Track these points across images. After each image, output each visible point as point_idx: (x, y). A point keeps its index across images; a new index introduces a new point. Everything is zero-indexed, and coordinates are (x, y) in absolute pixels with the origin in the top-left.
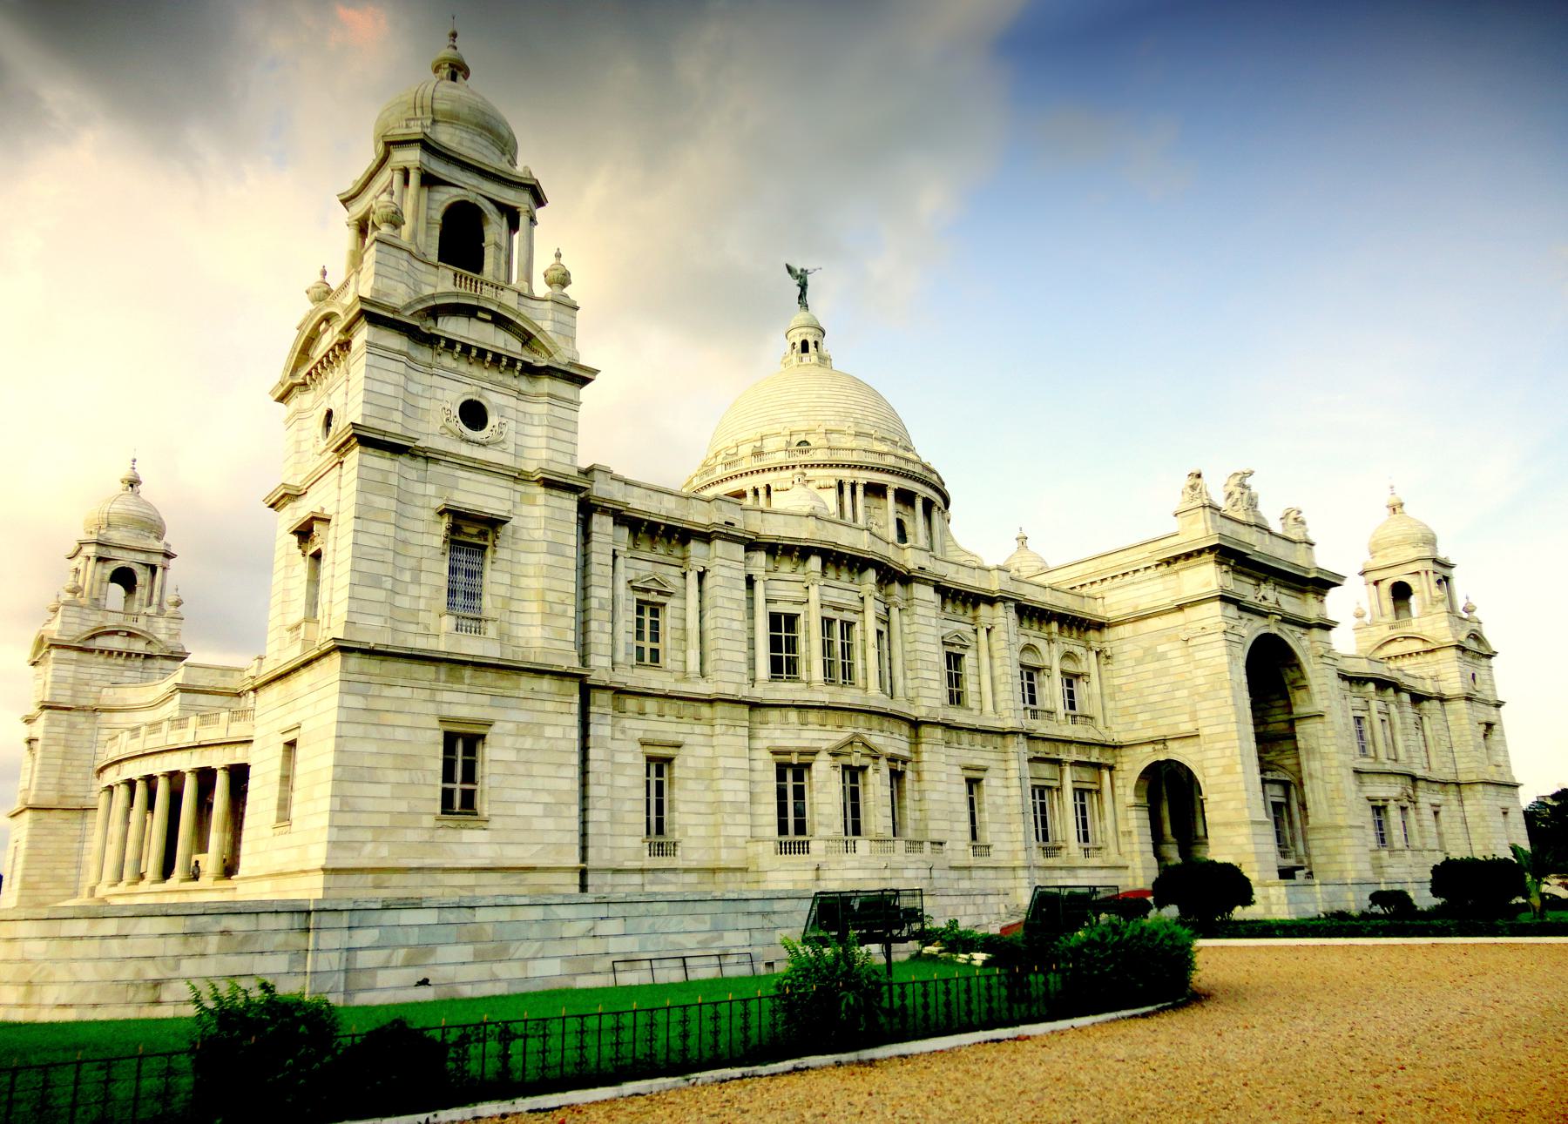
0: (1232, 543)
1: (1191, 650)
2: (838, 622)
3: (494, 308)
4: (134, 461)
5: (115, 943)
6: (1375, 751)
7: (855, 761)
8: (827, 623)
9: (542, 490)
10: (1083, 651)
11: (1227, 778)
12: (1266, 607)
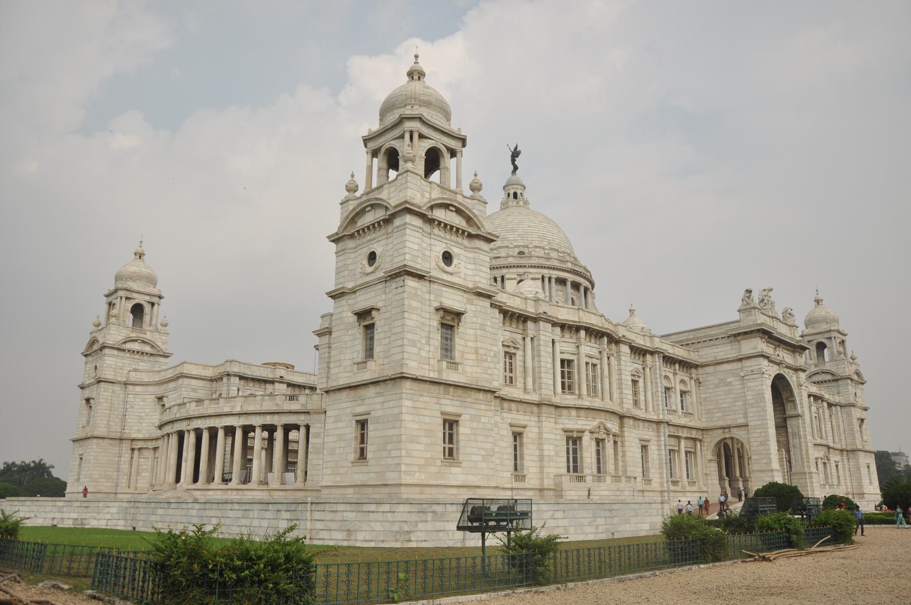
1: (745, 382)
2: (590, 364)
3: (457, 205)
4: (141, 242)
5: (389, 514)
7: (602, 436)
8: (587, 363)
9: (476, 297)
10: (689, 379)
11: (762, 448)
12: (778, 360)
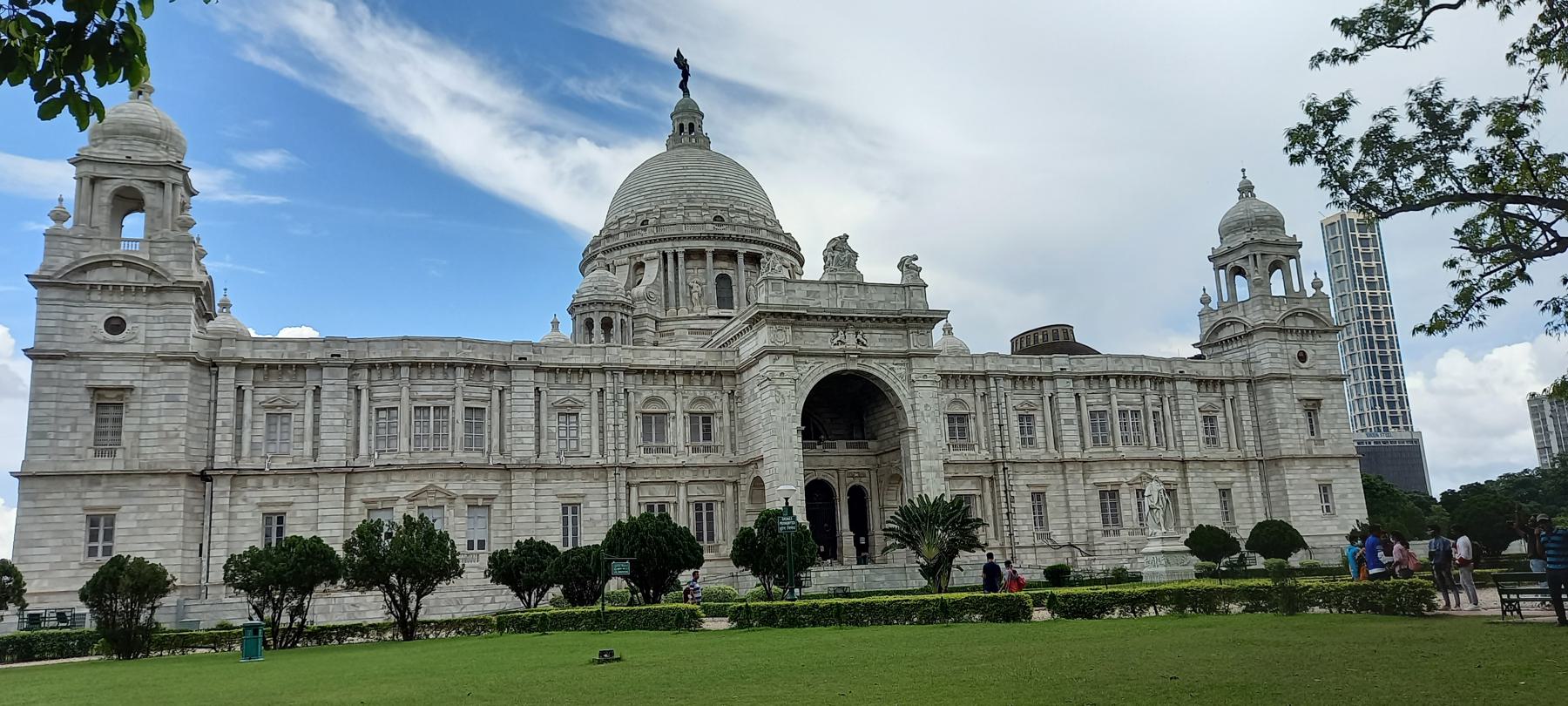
0: (777, 308)
2: (432, 408)
3: (122, 259)
6: (1114, 441)
9: (162, 363)
10: (719, 394)
